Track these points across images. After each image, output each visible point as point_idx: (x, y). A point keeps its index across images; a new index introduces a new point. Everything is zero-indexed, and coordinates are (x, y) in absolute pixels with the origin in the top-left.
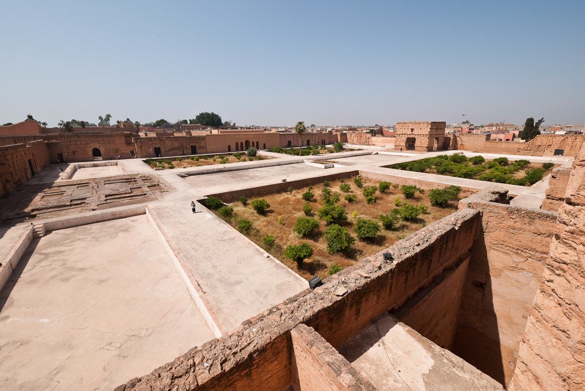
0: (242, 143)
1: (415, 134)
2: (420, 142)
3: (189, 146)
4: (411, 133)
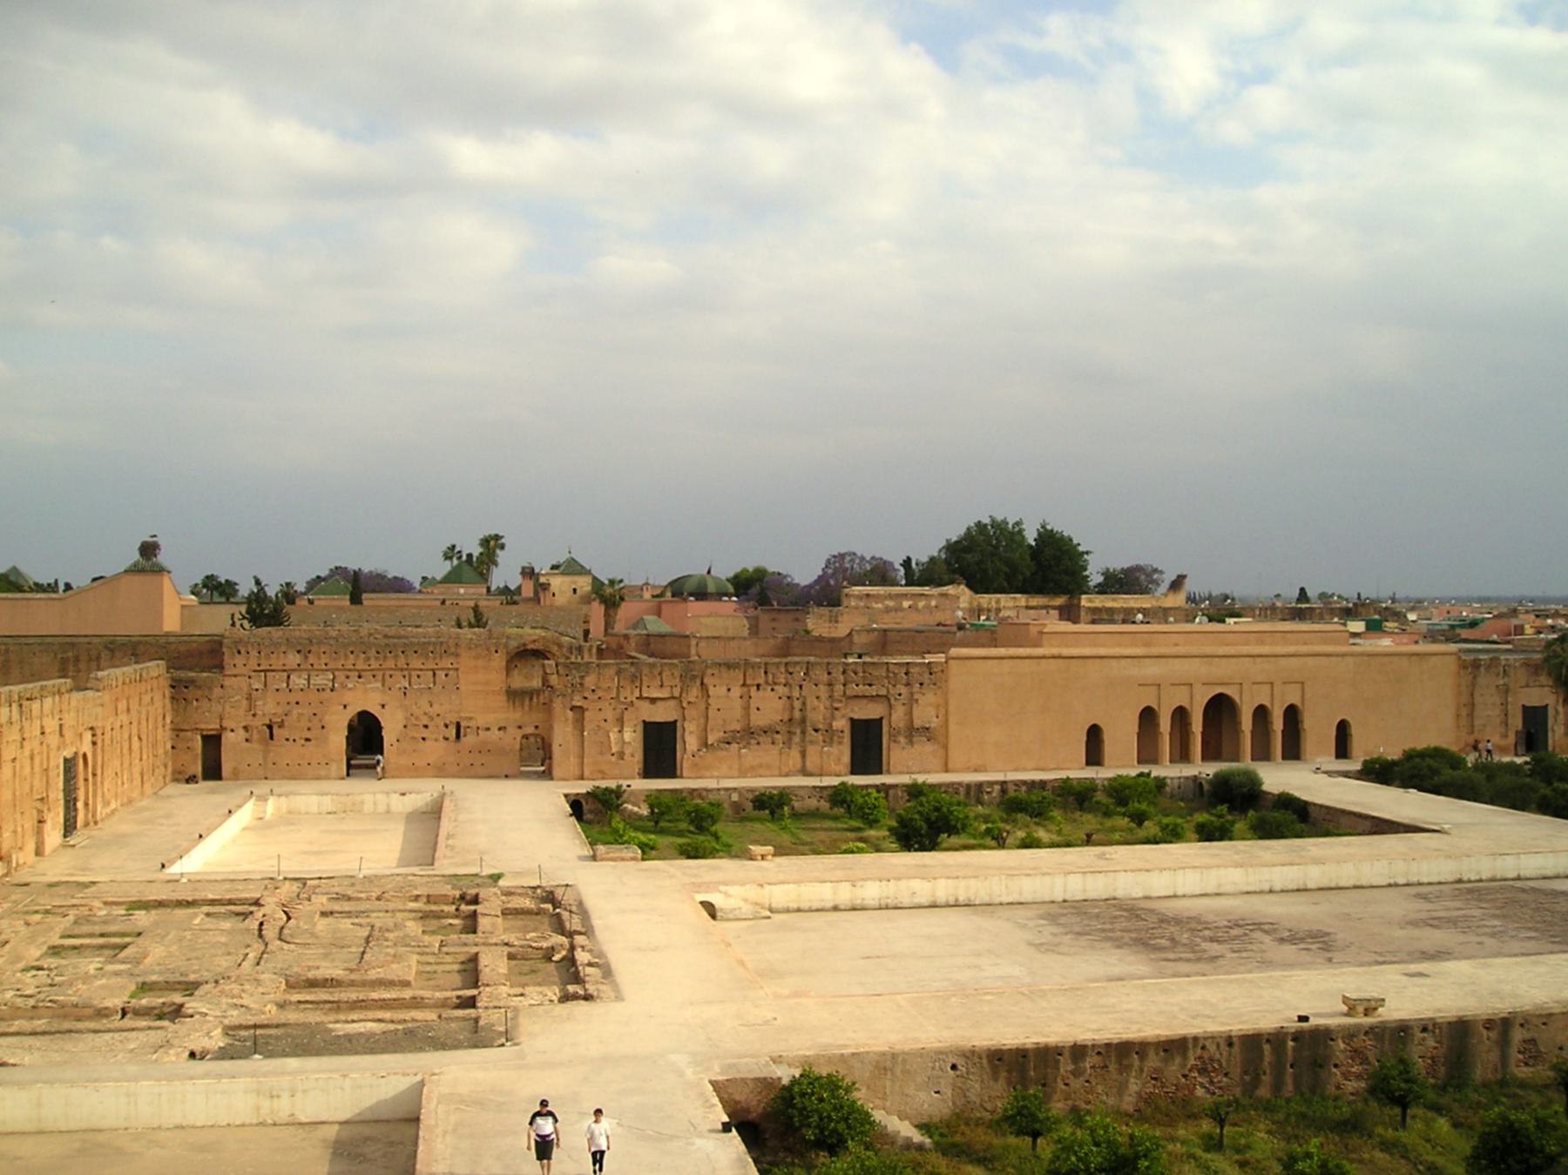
0: (1181, 715)
3: (841, 724)
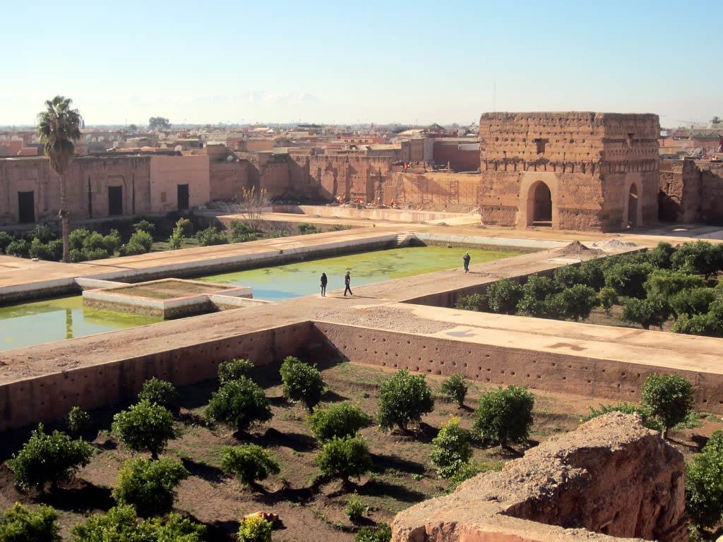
1: (553, 158)
2: (575, 193)
4: (536, 157)
